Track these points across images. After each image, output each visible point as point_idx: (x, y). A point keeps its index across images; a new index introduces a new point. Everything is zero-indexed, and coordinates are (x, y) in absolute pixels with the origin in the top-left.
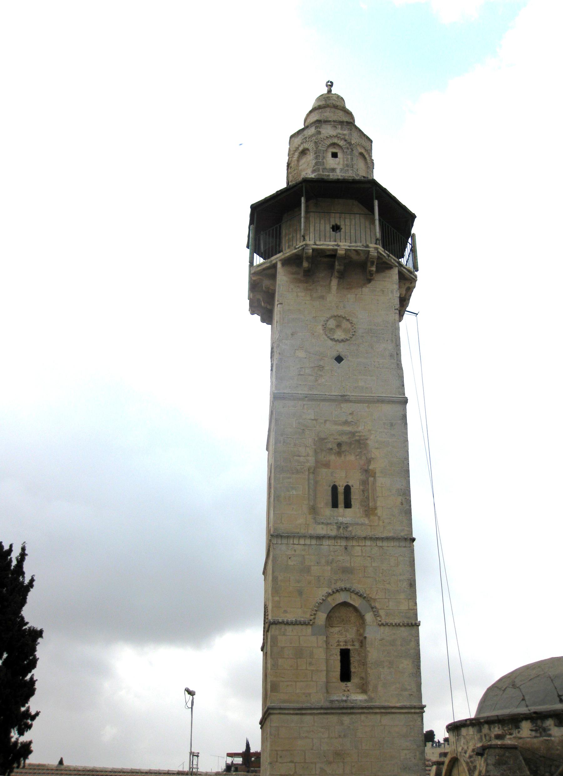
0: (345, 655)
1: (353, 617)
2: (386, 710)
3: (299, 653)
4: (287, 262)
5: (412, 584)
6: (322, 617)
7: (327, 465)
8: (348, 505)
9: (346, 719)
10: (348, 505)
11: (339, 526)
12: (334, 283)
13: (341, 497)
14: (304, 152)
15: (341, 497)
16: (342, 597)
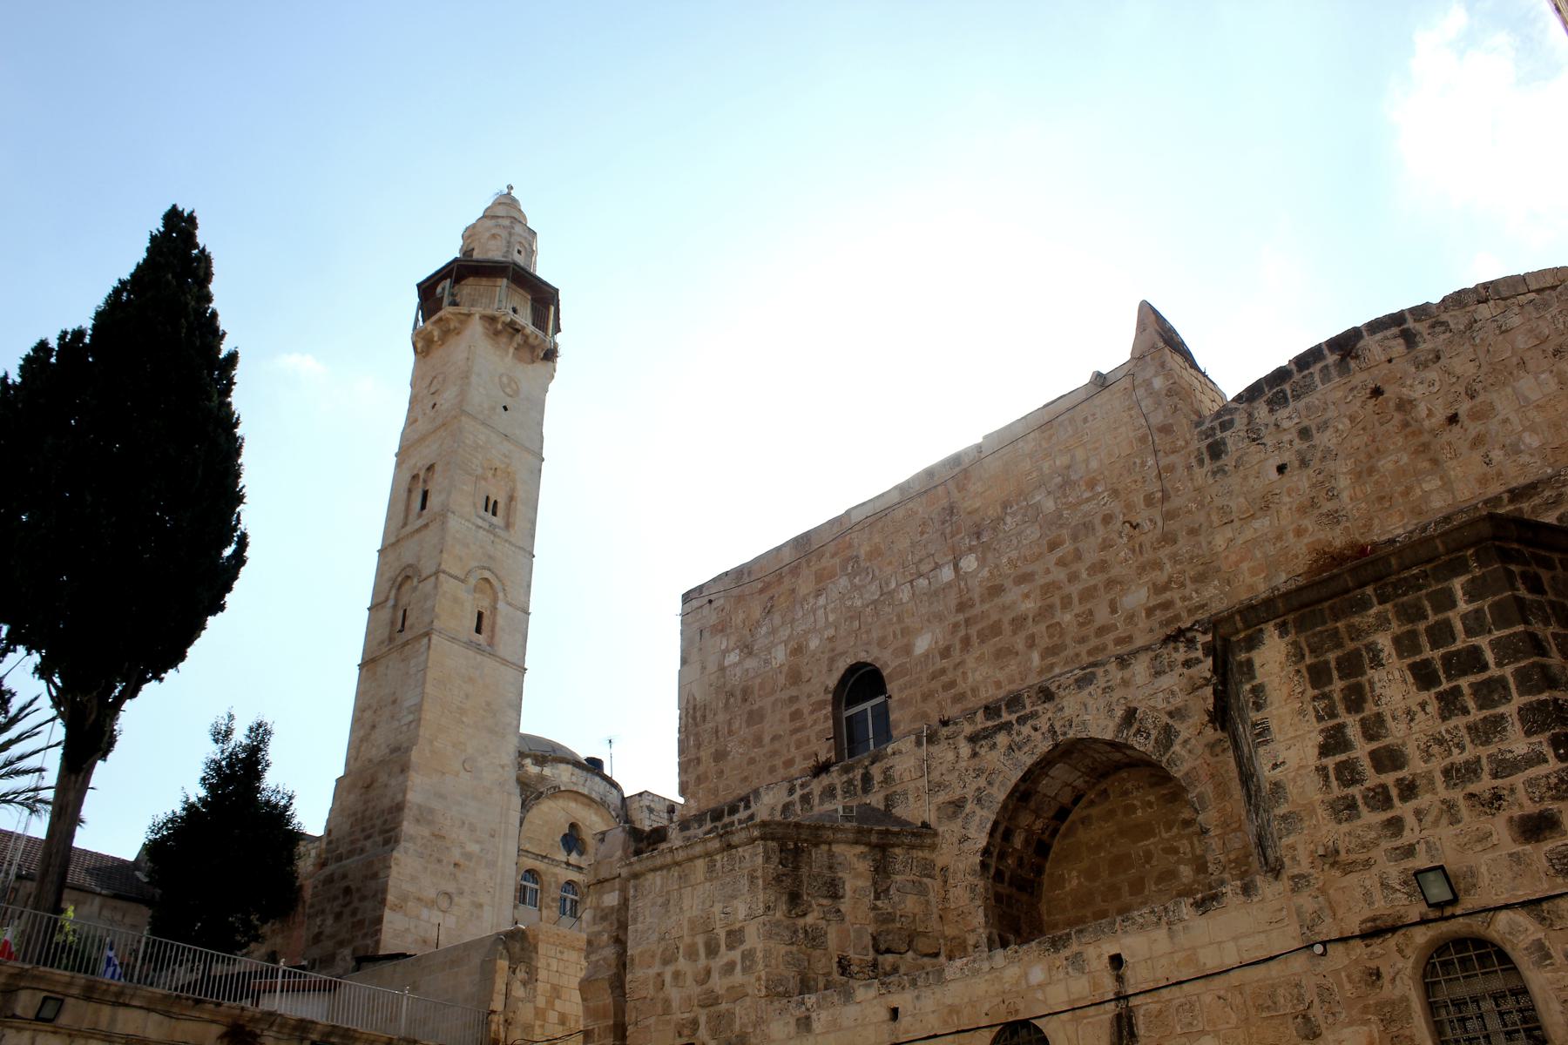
0: (480, 615)
1: (489, 591)
2: (505, 662)
3: (456, 600)
4: (483, 317)
5: (529, 586)
6: (472, 581)
7: (485, 479)
8: (494, 514)
9: (479, 657)
10: (494, 514)
11: (491, 525)
12: (511, 350)
13: (492, 507)
14: (494, 236)
15: (492, 507)
16: (487, 574)
